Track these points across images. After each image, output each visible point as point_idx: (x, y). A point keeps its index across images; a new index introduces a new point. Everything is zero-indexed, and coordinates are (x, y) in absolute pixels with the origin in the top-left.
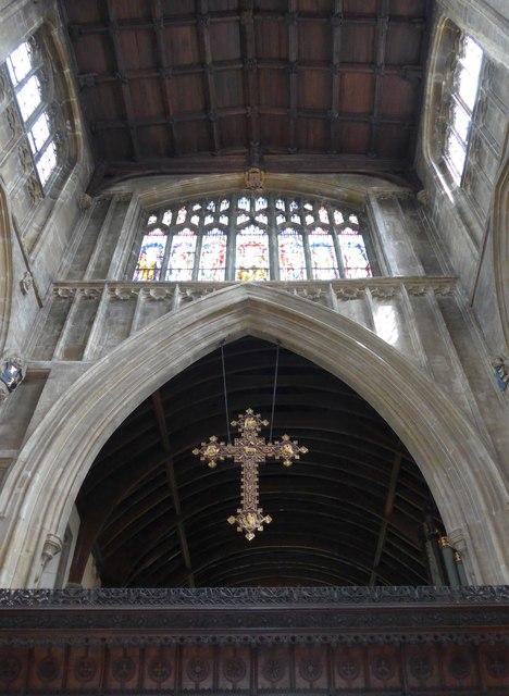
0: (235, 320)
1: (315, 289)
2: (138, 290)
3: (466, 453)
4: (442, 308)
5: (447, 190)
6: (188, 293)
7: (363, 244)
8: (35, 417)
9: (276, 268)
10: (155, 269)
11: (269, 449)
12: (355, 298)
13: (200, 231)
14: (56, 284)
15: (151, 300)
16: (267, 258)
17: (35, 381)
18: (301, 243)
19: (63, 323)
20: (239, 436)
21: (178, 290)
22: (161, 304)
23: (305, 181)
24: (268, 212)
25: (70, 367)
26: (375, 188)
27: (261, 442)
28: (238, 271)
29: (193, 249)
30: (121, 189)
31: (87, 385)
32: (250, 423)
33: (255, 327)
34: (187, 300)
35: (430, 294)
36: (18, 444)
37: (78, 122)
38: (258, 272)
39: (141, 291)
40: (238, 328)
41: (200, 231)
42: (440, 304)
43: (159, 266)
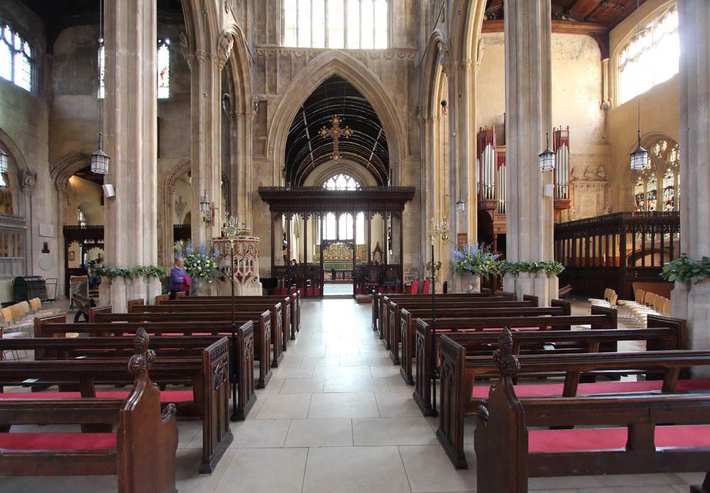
0: (330, 69)
1: (361, 54)
6: (311, 53)
8: (268, 124)
14: (256, 47)
17: (263, 106)
19: (264, 71)
20: (332, 126)
25: (273, 99)
27: (339, 128)
31: (282, 107)
32: (336, 121)
33: (338, 72)
36: (266, 135)
40: (331, 73)
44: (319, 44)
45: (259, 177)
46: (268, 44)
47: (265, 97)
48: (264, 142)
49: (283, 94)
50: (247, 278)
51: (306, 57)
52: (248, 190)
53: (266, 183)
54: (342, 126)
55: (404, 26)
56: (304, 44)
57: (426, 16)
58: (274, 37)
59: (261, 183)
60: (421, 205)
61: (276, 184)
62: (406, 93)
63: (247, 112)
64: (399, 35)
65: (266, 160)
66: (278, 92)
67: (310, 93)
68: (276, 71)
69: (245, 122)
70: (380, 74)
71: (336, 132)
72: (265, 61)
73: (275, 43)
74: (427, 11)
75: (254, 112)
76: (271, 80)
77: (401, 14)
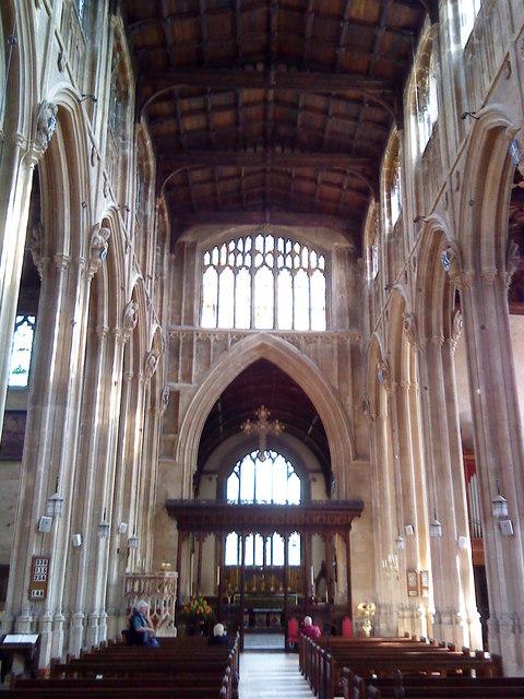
1: (293, 337)
3: (343, 438)
4: (352, 352)
5: (369, 279)
11: (270, 427)
13: (236, 270)
17: (175, 396)
19: (178, 357)
23: (296, 230)
24: (275, 253)
26: (336, 244)
30: (187, 238)
32: (263, 413)
34: (233, 342)
35: (348, 341)
36: (177, 432)
37: (166, 215)
40: (257, 357)
41: (236, 270)
42: (352, 346)
44: (243, 325)
45: (164, 485)
46: (184, 327)
47: (177, 386)
48: (173, 443)
49: (199, 382)
50: (164, 621)
51: (226, 340)
52: (151, 503)
53: (174, 495)
54: (270, 419)
55: (346, 306)
56: (226, 324)
57: (370, 302)
58: (190, 319)
59: (167, 492)
60: (372, 521)
61: (185, 496)
62: (350, 382)
63: (157, 407)
64: (340, 316)
65: (175, 464)
66: (193, 379)
67: (230, 380)
68: (191, 356)
69: (154, 418)
70: (316, 360)
71: (263, 426)
72: (178, 346)
73: (192, 324)
74: (370, 296)
75: (165, 407)
76: (184, 367)
77: (341, 293)
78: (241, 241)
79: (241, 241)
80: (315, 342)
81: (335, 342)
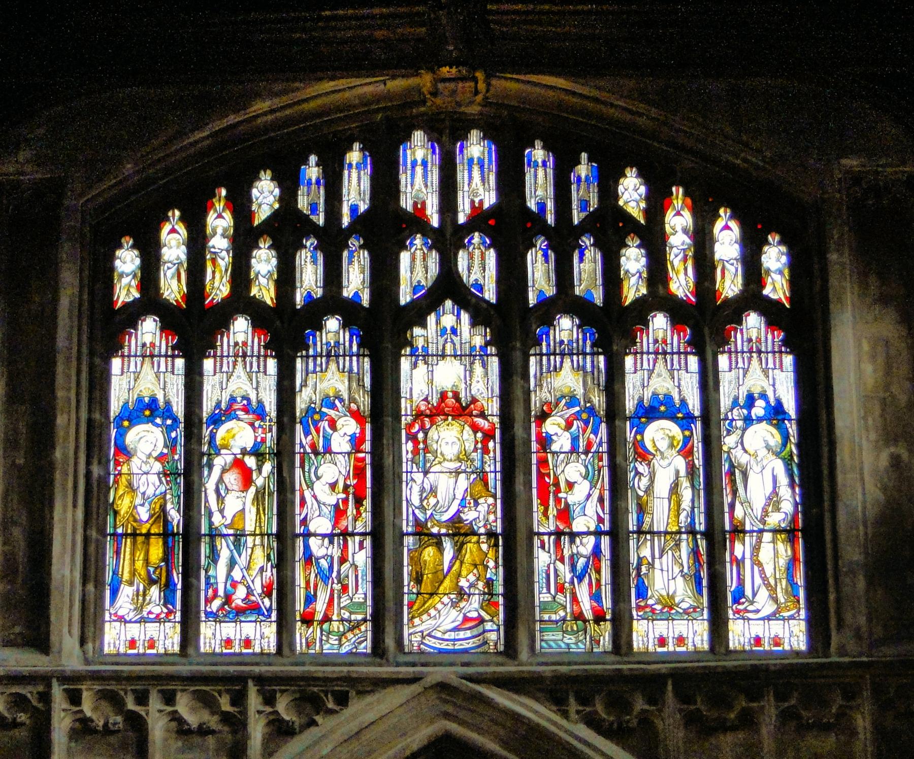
2: (142, 700)
6: (283, 706)
7: (790, 405)
9: (521, 535)
10: (167, 535)
12: (734, 728)
15: (182, 730)
16: (495, 480)
18: (598, 400)
21: (254, 700)
22: (211, 740)
28: (409, 541)
29: (270, 439)
38: (470, 546)
39: (155, 703)
43: (175, 517)
78: (312, 171)
79: (312, 171)
80: (748, 721)
81: (862, 722)
